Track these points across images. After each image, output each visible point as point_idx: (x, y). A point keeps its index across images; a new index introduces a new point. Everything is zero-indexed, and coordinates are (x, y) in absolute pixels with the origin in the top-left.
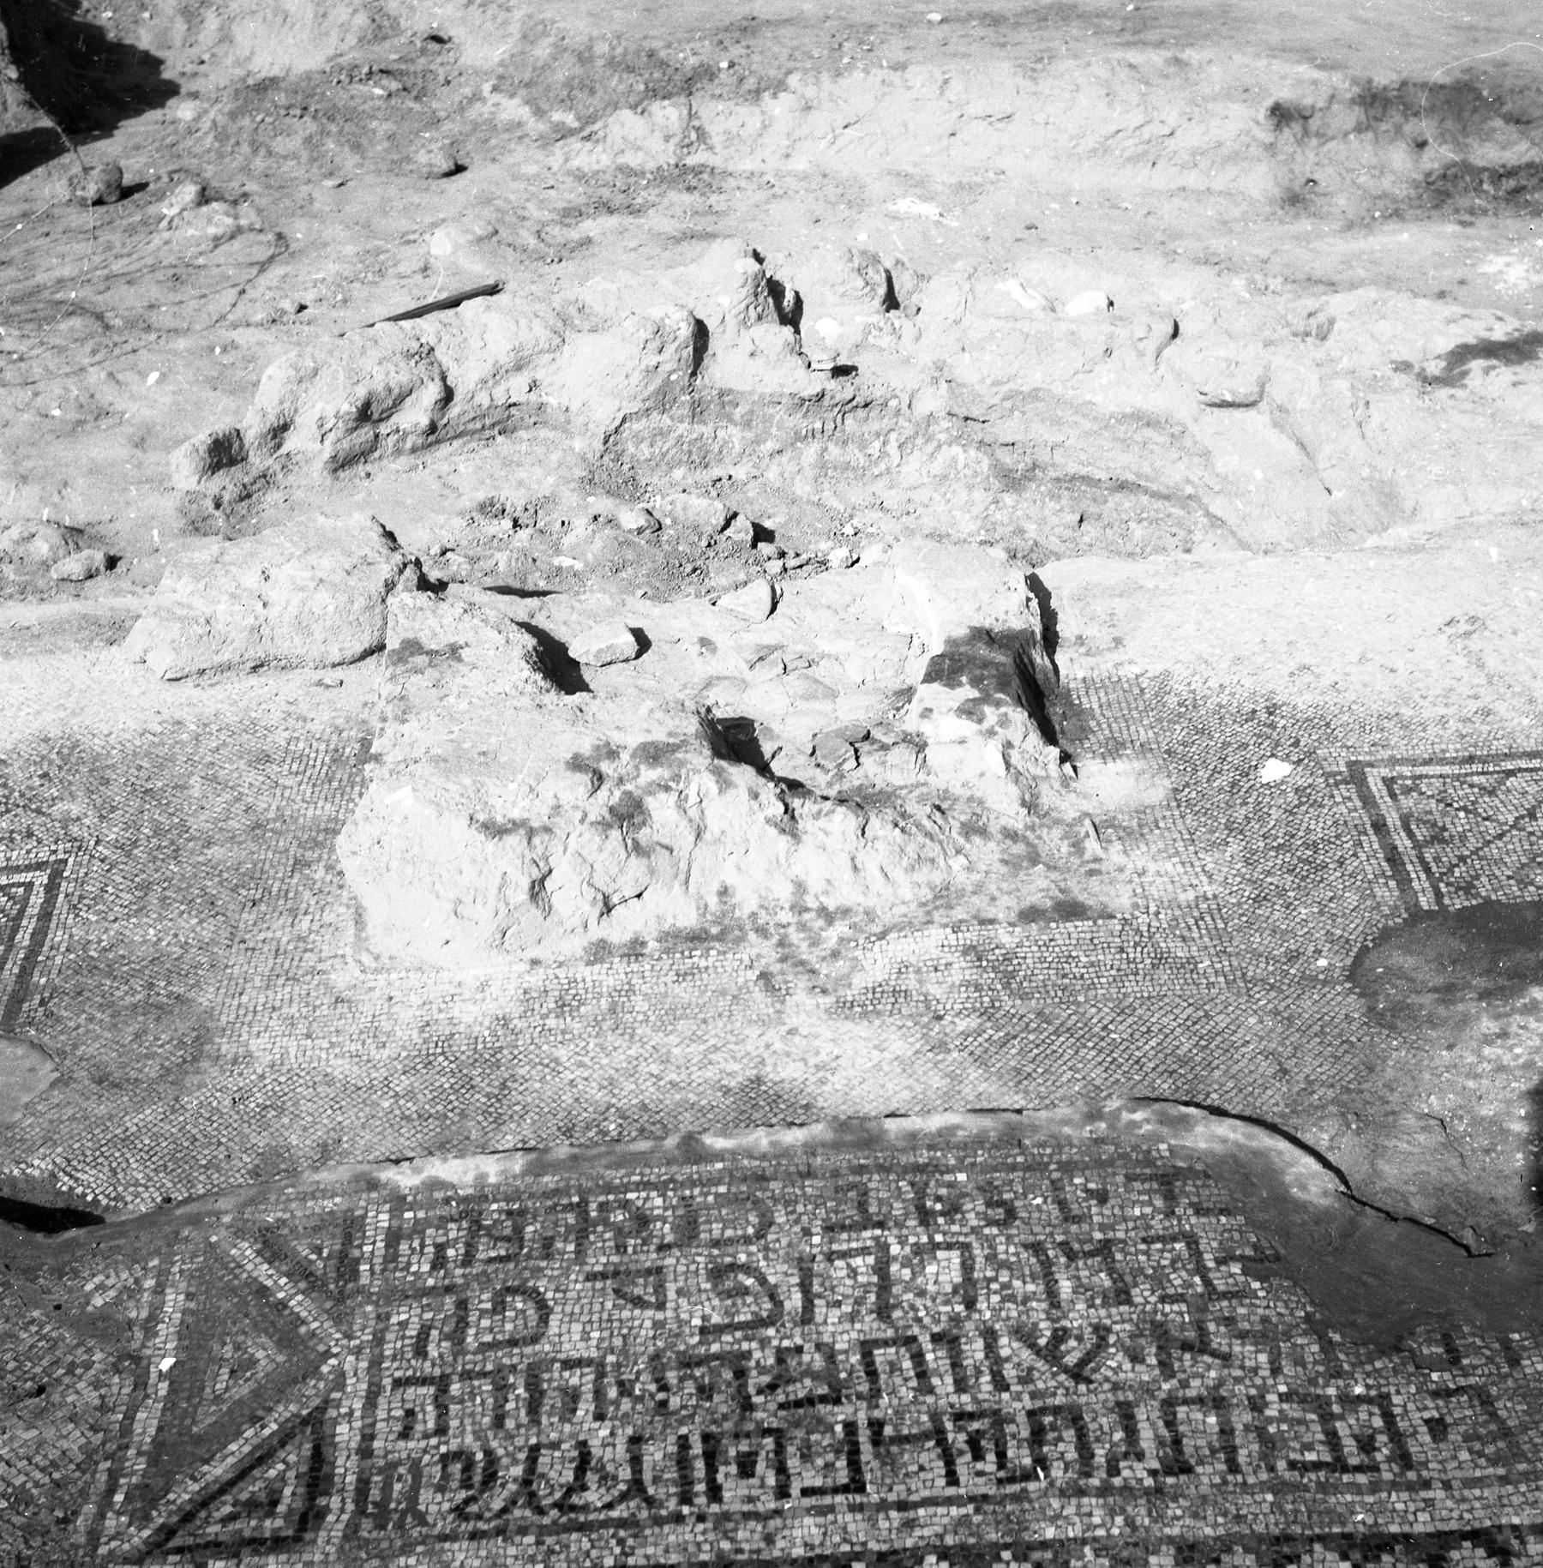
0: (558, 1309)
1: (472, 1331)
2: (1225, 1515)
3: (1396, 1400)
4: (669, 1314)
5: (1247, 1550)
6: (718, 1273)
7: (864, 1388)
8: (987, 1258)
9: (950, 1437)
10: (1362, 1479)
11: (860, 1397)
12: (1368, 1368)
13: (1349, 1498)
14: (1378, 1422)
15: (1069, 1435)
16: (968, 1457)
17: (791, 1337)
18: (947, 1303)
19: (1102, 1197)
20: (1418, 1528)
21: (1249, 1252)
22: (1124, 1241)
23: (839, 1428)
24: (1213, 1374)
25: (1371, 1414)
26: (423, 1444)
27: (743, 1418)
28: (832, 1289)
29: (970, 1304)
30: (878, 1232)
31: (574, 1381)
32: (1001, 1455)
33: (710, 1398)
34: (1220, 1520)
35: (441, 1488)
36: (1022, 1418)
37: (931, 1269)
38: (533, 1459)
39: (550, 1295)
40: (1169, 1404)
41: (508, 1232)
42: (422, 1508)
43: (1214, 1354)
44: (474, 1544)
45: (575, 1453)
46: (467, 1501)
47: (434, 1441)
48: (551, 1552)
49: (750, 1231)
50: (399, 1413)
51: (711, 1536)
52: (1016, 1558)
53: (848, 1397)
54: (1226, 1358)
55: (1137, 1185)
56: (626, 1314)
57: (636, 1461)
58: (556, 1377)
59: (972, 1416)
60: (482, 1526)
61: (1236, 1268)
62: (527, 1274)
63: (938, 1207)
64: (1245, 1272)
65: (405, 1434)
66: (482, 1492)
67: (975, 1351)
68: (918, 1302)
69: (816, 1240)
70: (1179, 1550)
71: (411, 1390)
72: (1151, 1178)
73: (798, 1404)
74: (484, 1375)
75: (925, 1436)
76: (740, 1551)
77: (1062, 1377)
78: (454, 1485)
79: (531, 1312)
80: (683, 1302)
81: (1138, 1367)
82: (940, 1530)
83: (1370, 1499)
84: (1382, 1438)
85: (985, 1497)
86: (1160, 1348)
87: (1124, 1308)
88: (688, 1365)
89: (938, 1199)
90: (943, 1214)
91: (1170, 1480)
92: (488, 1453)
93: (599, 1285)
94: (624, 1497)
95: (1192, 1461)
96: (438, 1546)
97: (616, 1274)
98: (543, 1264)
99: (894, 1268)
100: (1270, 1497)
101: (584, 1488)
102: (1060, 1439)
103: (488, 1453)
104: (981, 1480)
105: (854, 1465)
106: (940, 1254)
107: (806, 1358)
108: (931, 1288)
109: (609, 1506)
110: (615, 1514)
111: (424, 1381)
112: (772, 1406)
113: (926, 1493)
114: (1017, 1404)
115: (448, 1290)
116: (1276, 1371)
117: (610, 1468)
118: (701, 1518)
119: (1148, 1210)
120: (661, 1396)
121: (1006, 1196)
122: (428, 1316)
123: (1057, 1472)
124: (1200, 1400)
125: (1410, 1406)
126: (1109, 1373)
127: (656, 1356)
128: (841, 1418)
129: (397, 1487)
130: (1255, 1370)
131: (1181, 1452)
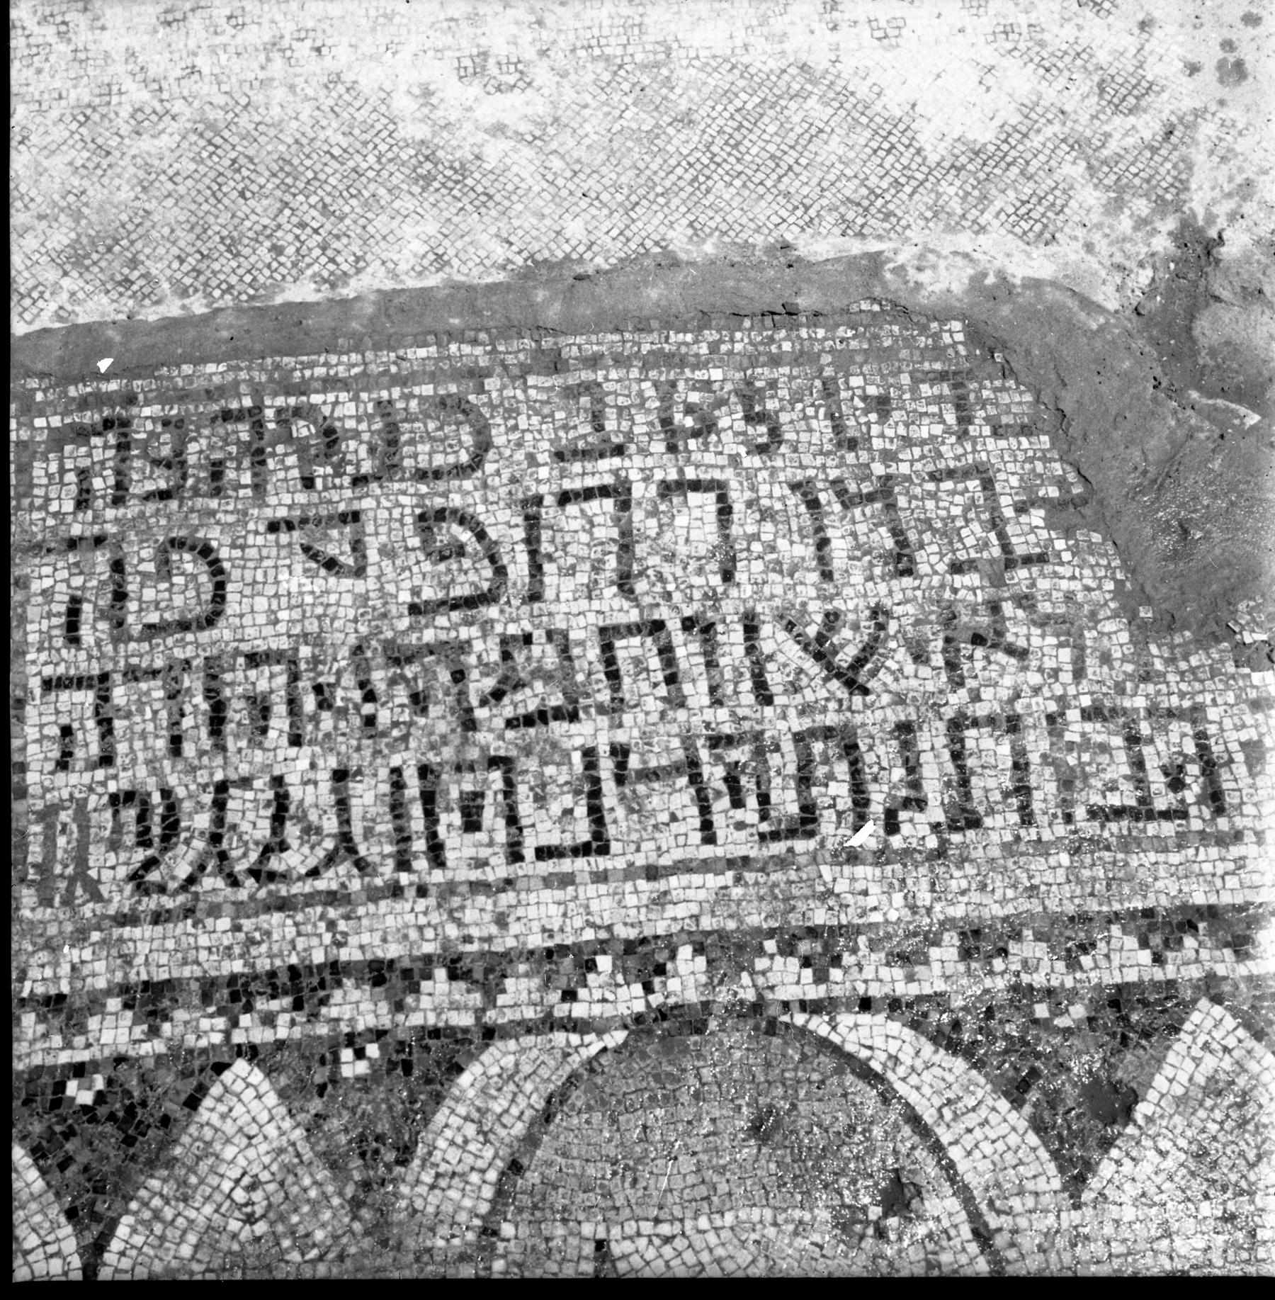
0: (236, 574)
1: (132, 606)
2: (1014, 887)
3: (1212, 714)
4: (372, 584)
5: (1039, 937)
6: (428, 520)
7: (605, 696)
8: (749, 504)
9: (706, 770)
10: (1168, 828)
11: (601, 710)
12: (1183, 665)
13: (1152, 857)
14: (1190, 748)
15: (842, 769)
16: (725, 802)
17: (516, 620)
18: (700, 571)
19: (882, 406)
20: (1226, 899)
21: (1053, 492)
22: (908, 478)
23: (577, 757)
24: (1008, 681)
25: (1184, 735)
26: (87, 778)
27: (465, 742)
28: (566, 545)
29: (728, 576)
30: (616, 462)
31: (263, 686)
32: (764, 799)
33: (424, 711)
34: (1010, 893)
35: (114, 845)
36: (788, 746)
37: (681, 520)
38: (220, 805)
39: (224, 553)
40: (957, 725)
41: (166, 451)
42: (93, 873)
43: (1011, 651)
44: (159, 929)
45: (270, 795)
46: (150, 864)
47: (100, 774)
48: (251, 942)
49: (464, 458)
50: (55, 731)
51: (435, 918)
52: (782, 952)
53: (586, 709)
54: (1021, 654)
55: (925, 389)
56: (319, 585)
57: (342, 805)
58: (238, 682)
59: (730, 741)
60: (168, 903)
61: (1037, 517)
62: (194, 519)
63: (689, 422)
64: (1049, 527)
65: (63, 764)
66: (164, 850)
67: (732, 641)
68: (667, 569)
69: (543, 473)
70: (963, 934)
71: (64, 696)
72: (942, 376)
73: (529, 721)
74: (154, 673)
75: (676, 769)
76: (468, 939)
77: (835, 684)
78: (130, 839)
79: (204, 578)
80: (386, 563)
81: (925, 671)
82: (694, 909)
83: (1175, 858)
84: (1193, 769)
85: (746, 859)
86: (948, 640)
87: (907, 581)
88: (397, 662)
89: (689, 409)
90: (696, 434)
91: (956, 838)
92: (166, 793)
93: (284, 538)
94: (331, 860)
95: (981, 810)
96: (116, 932)
97: (304, 521)
98: (214, 504)
99: (638, 515)
100: (1064, 858)
101: (283, 847)
102: (831, 777)
103: (166, 793)
104: (742, 835)
105: (596, 812)
106: (694, 498)
107: (536, 650)
108: (682, 550)
109: (314, 873)
110: (321, 884)
111: (79, 683)
112: (499, 723)
113: (678, 854)
114: (781, 723)
115: (99, 541)
116: (1079, 673)
117: (313, 816)
118: (422, 891)
119: (938, 429)
120: (368, 709)
121: (771, 405)
122: (77, 581)
123: (827, 823)
124: (991, 721)
125: (1228, 723)
126: (889, 679)
127: (358, 650)
128: (578, 741)
129: (61, 841)
130: (1055, 673)
131: (967, 796)
